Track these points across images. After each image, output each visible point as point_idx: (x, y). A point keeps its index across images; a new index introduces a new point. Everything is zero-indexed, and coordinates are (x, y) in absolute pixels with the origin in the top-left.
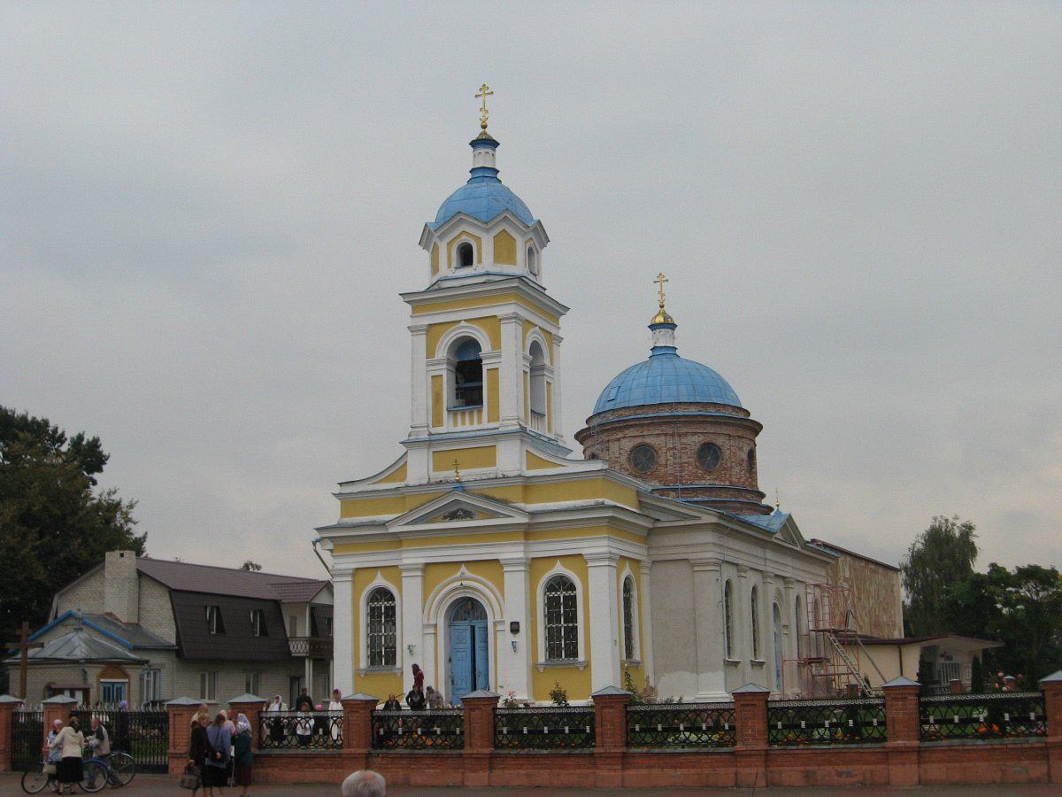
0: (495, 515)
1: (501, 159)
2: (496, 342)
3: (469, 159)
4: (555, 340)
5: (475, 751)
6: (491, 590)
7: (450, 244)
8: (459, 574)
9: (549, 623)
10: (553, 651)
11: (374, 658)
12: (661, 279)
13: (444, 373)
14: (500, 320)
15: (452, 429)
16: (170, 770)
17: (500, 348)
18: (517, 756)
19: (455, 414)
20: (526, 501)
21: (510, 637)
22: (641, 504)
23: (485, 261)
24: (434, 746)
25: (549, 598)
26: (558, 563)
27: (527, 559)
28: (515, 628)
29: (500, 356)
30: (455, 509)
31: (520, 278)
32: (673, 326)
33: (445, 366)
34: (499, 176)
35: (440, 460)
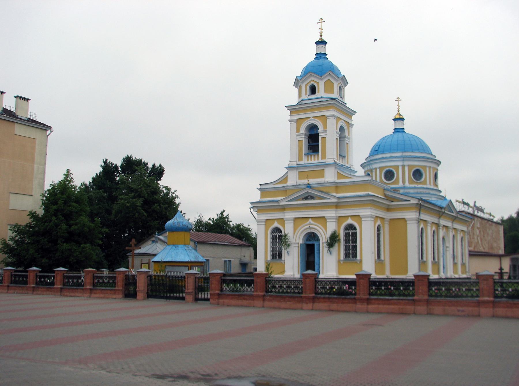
0: (324, 198)
1: (329, 50)
2: (325, 126)
3: (313, 50)
4: (350, 125)
5: (307, 295)
6: (322, 230)
7: (306, 85)
8: (308, 223)
9: (345, 243)
10: (347, 255)
11: (273, 256)
12: (398, 100)
13: (303, 139)
14: (326, 117)
15: (306, 162)
16: (186, 299)
17: (327, 129)
18: (324, 298)
19: (308, 156)
20: (337, 193)
22: (385, 195)
23: (321, 92)
24: (275, 292)
25: (345, 233)
26: (350, 218)
27: (336, 216)
30: (307, 195)
31: (335, 99)
32: (403, 119)
33: (304, 136)
34: (327, 56)
35: (301, 175)
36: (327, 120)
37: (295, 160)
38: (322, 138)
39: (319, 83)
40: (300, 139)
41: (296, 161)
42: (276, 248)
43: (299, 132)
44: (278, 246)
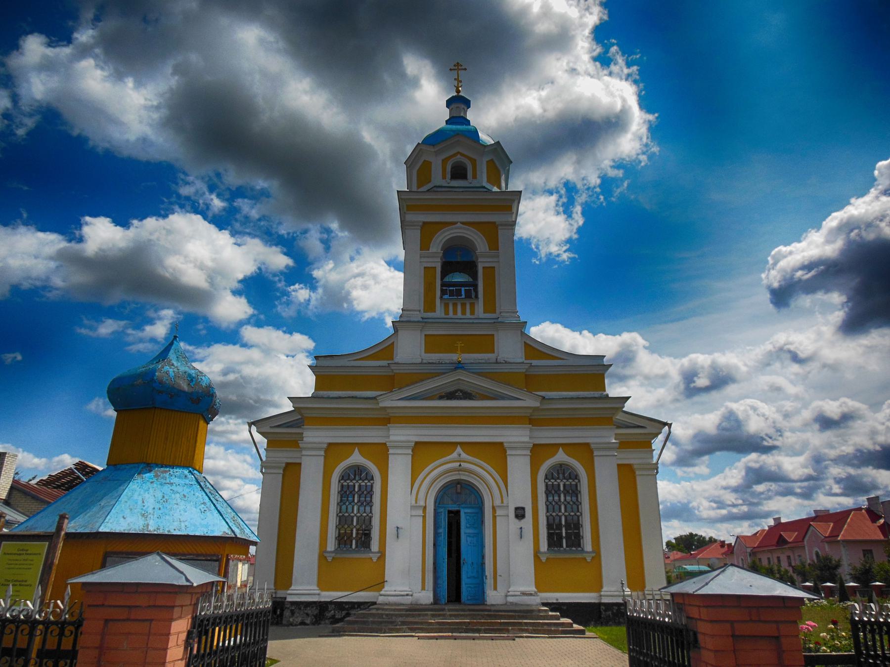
2: (494, 244)
7: (445, 161)
8: (454, 455)
10: (554, 540)
11: (343, 540)
17: (498, 250)
21: (514, 524)
28: (520, 513)
29: (498, 256)
30: (452, 389)
35: (432, 344)
36: (500, 232)
37: (419, 309)
38: (483, 268)
39: (475, 160)
40: (429, 265)
41: (420, 311)
42: (353, 517)
43: (429, 250)
44: (359, 515)
